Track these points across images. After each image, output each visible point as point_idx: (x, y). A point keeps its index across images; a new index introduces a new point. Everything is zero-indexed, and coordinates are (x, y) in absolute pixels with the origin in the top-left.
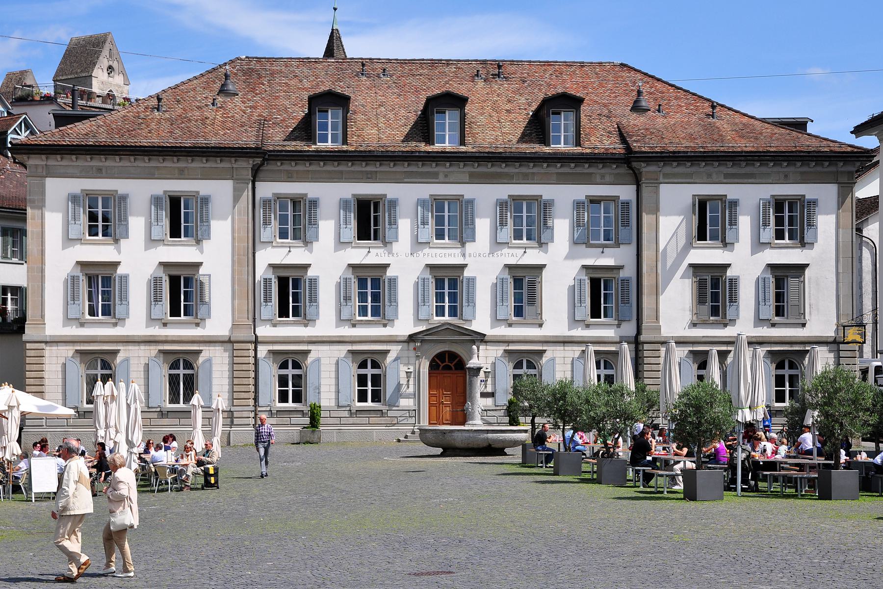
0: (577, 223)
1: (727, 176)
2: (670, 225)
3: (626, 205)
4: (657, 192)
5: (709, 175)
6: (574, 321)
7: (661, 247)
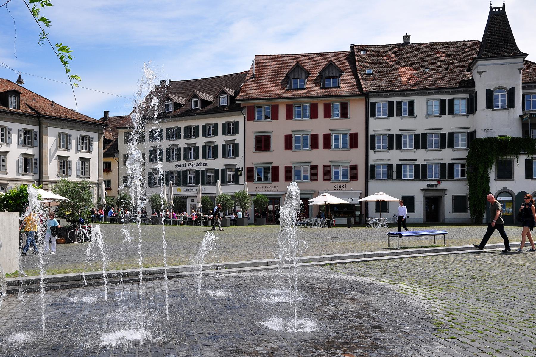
0: (19, 138)
1: (68, 127)
2: (51, 140)
3: (36, 133)
4: (47, 130)
5: (63, 126)
6: (18, 173)
7: (49, 149)
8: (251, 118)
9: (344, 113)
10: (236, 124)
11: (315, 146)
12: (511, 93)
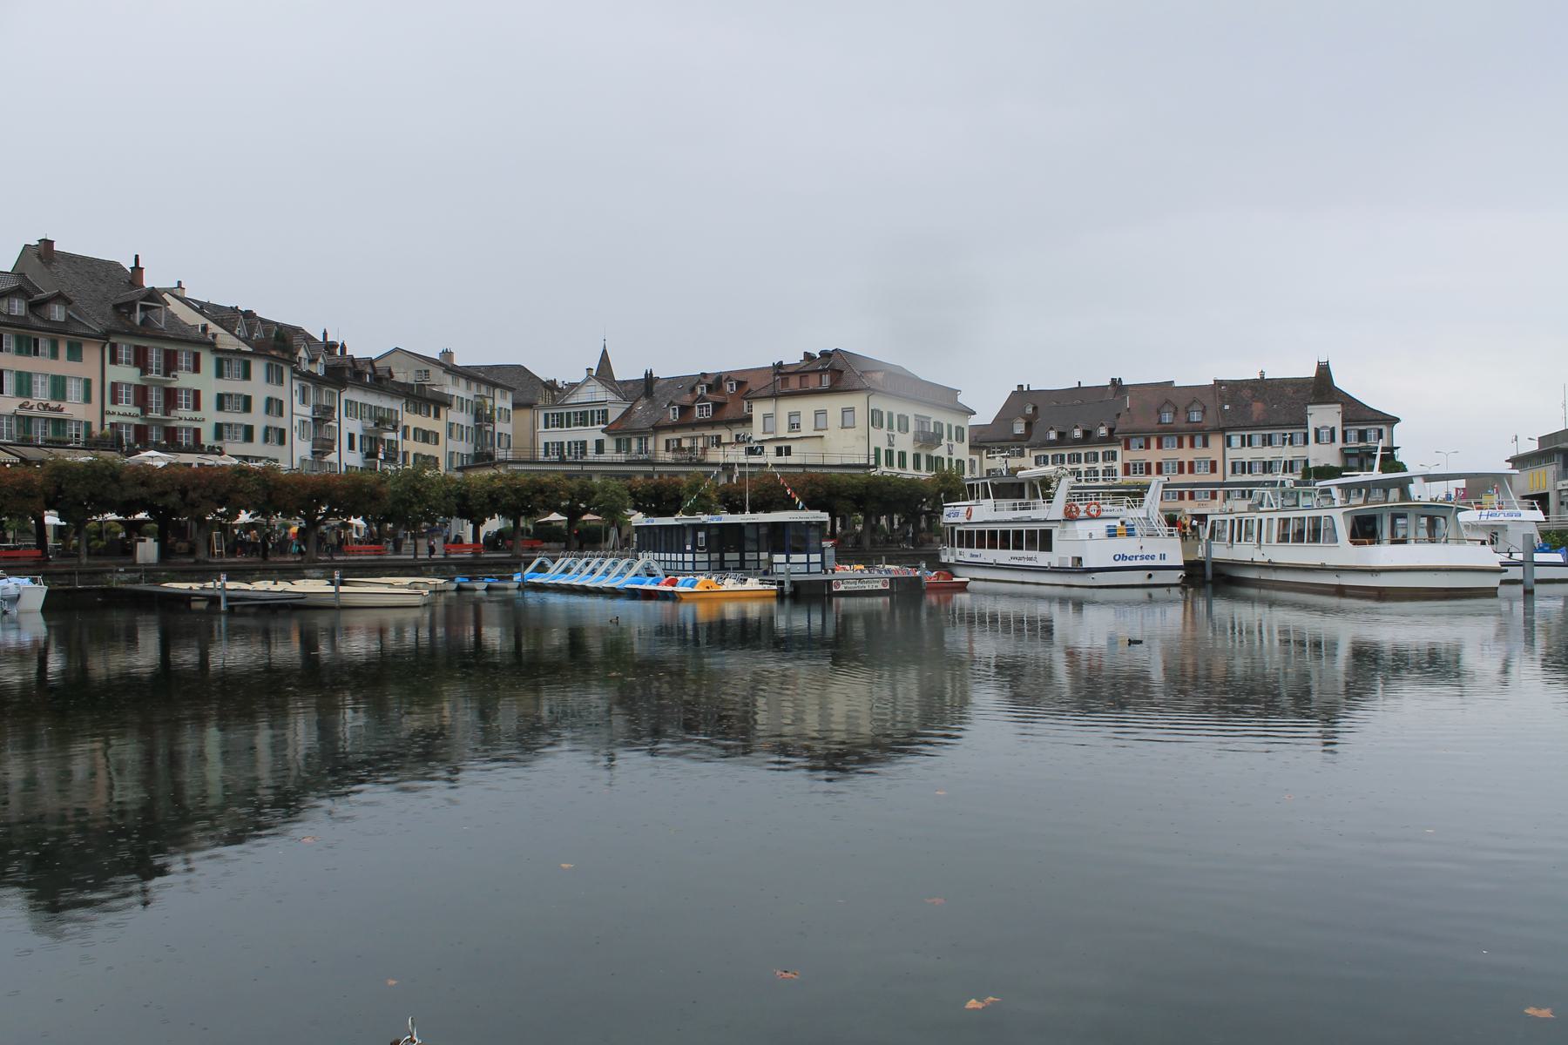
8: (1127, 447)
9: (1206, 444)
10: (1114, 453)
11: (1181, 471)
12: (1333, 431)
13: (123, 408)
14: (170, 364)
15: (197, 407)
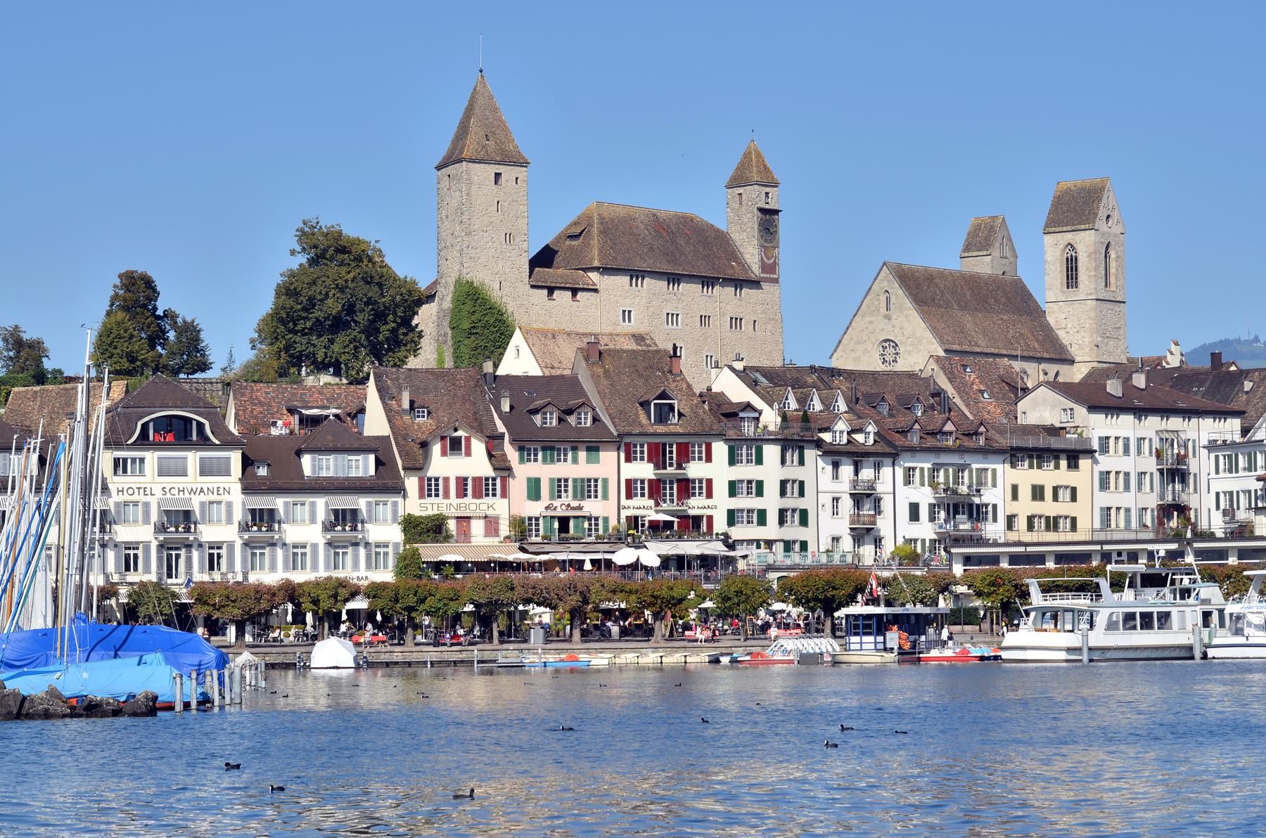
13: (638, 501)
14: (685, 455)
15: (710, 495)
